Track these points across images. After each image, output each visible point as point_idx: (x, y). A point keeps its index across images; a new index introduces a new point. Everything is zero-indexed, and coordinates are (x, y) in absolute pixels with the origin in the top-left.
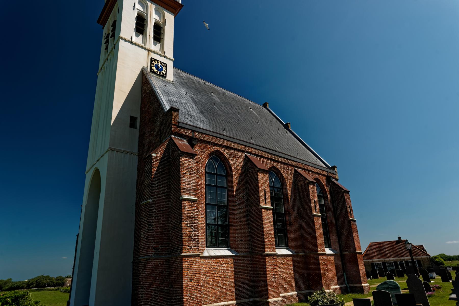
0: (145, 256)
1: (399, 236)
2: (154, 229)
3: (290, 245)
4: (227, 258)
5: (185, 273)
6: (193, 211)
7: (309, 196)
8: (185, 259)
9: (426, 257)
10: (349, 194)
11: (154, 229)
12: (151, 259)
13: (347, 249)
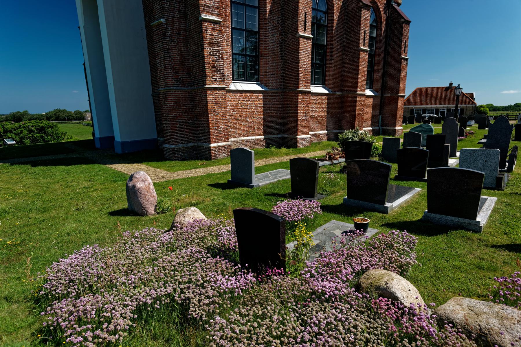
0: (165, 87)
2: (171, 57)
3: (327, 83)
4: (256, 93)
5: (210, 106)
6: (216, 35)
7: (359, 24)
8: (209, 92)
10: (409, 24)
11: (171, 57)
12: (172, 90)
13: (389, 92)
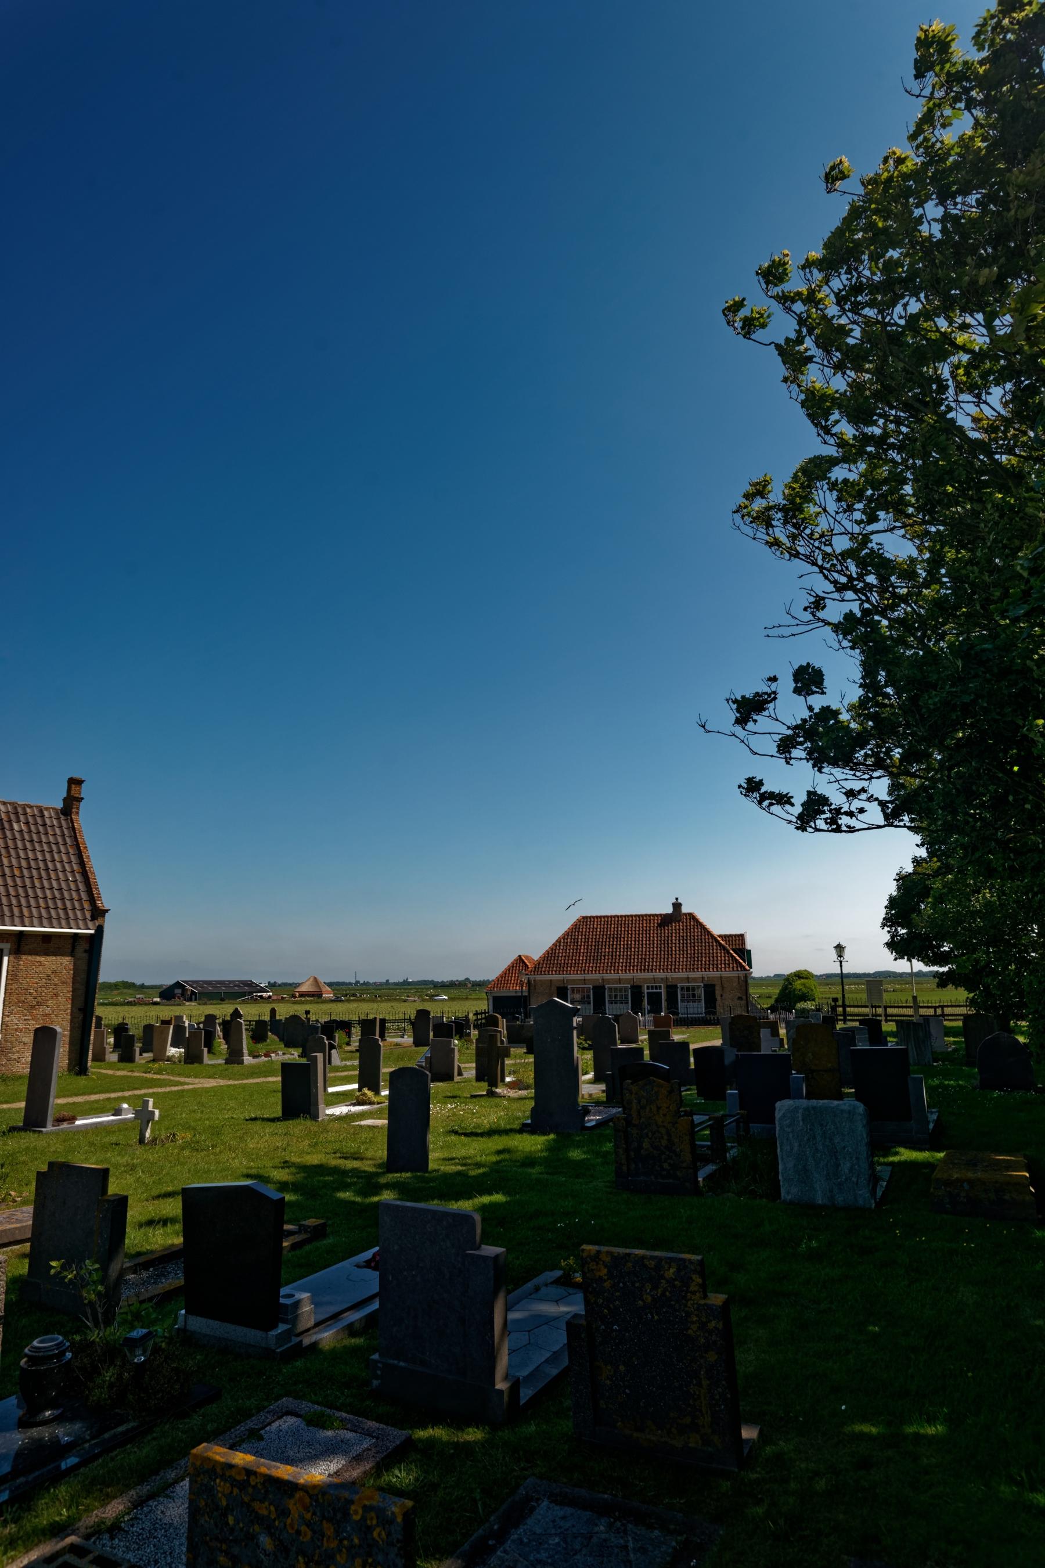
1: (677, 899)
9: (735, 974)
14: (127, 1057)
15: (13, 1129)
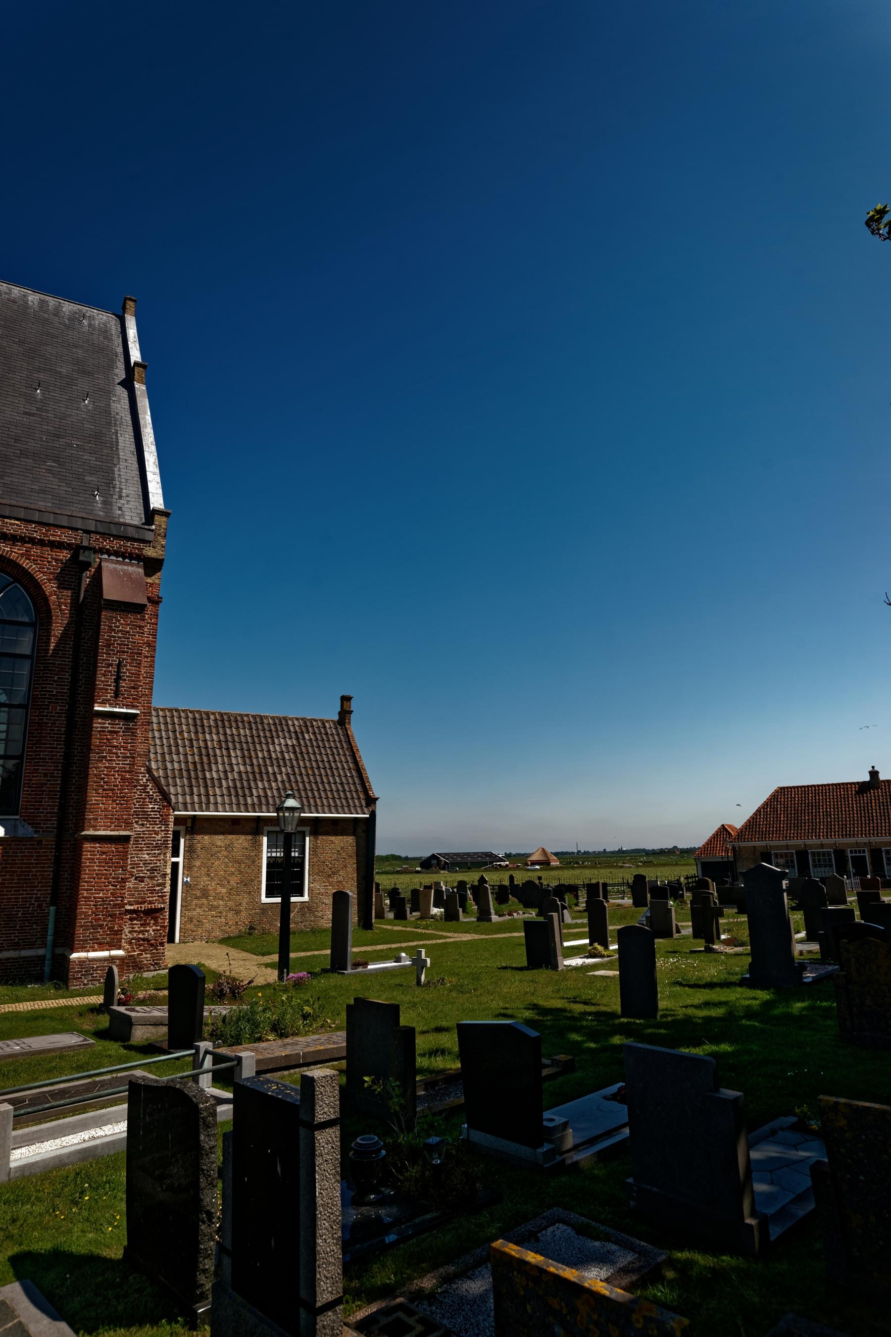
1: (873, 767)
14: (400, 916)
15: (324, 971)
